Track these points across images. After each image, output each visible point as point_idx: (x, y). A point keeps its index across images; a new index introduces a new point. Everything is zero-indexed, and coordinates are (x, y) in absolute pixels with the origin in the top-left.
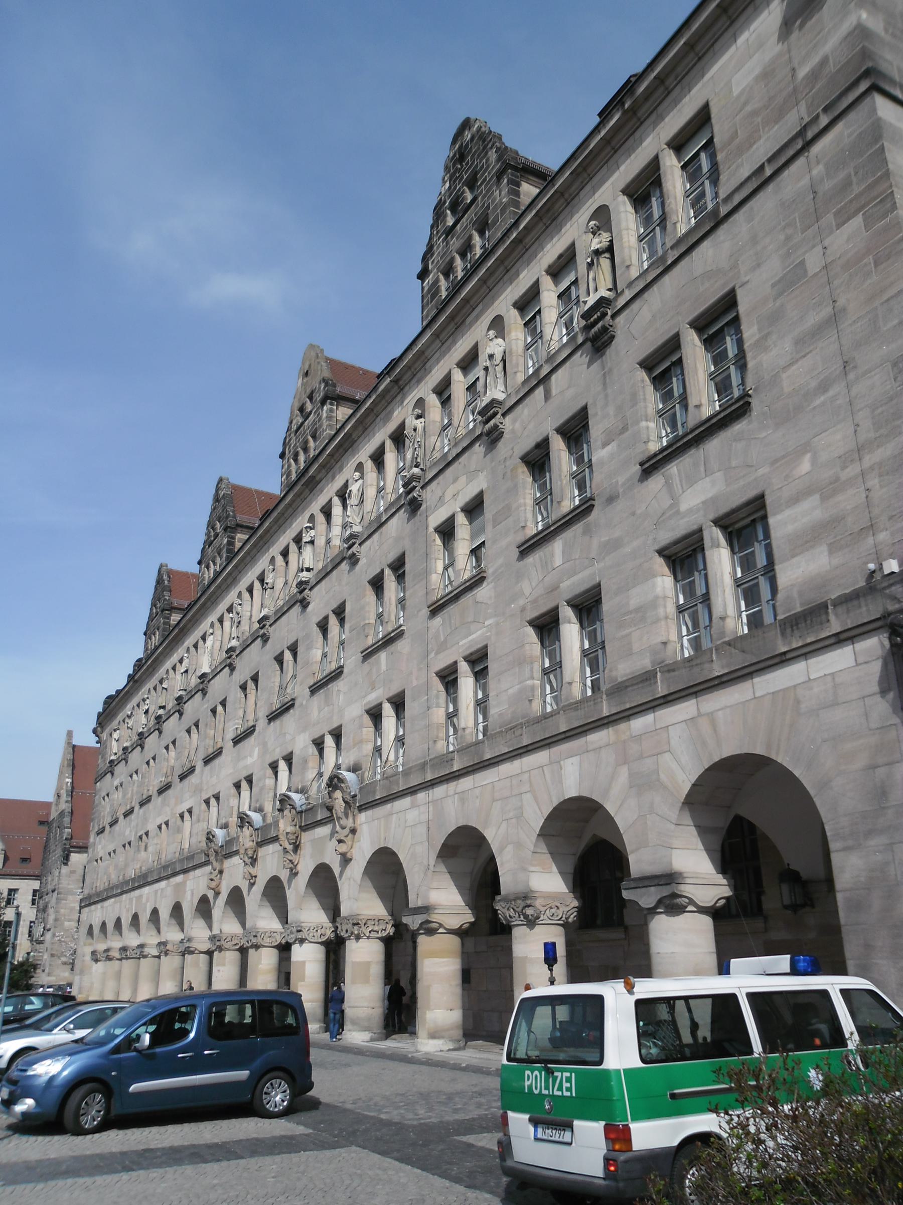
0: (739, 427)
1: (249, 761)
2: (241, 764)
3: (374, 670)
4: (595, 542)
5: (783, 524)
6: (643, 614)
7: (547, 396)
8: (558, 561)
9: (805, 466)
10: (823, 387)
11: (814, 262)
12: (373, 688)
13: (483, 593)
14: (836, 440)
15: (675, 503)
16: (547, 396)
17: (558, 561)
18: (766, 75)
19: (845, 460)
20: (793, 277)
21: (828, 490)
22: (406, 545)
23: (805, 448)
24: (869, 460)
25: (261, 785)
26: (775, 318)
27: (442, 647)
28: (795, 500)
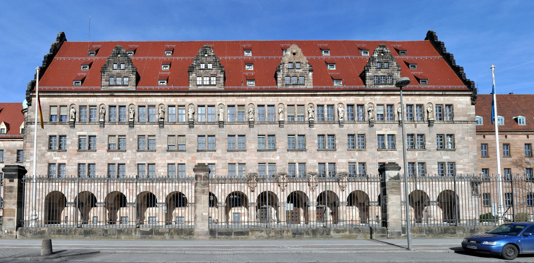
0: (453, 152)
1: (272, 159)
2: (264, 158)
3: (352, 155)
4: (425, 156)
5: (458, 166)
6: (434, 169)
7: (416, 127)
8: (417, 155)
9: (462, 161)
10: (465, 154)
11: (466, 138)
12: (352, 158)
13: (394, 152)
14: (466, 160)
15: (442, 157)
16: (416, 127)
17: (417, 155)
18: (462, 108)
19: (467, 163)
20: (463, 138)
21: (464, 165)
22: (367, 133)
23: (462, 159)
24: (470, 164)
25: (284, 167)
26: (460, 142)
27: (382, 158)
28: (460, 164)
